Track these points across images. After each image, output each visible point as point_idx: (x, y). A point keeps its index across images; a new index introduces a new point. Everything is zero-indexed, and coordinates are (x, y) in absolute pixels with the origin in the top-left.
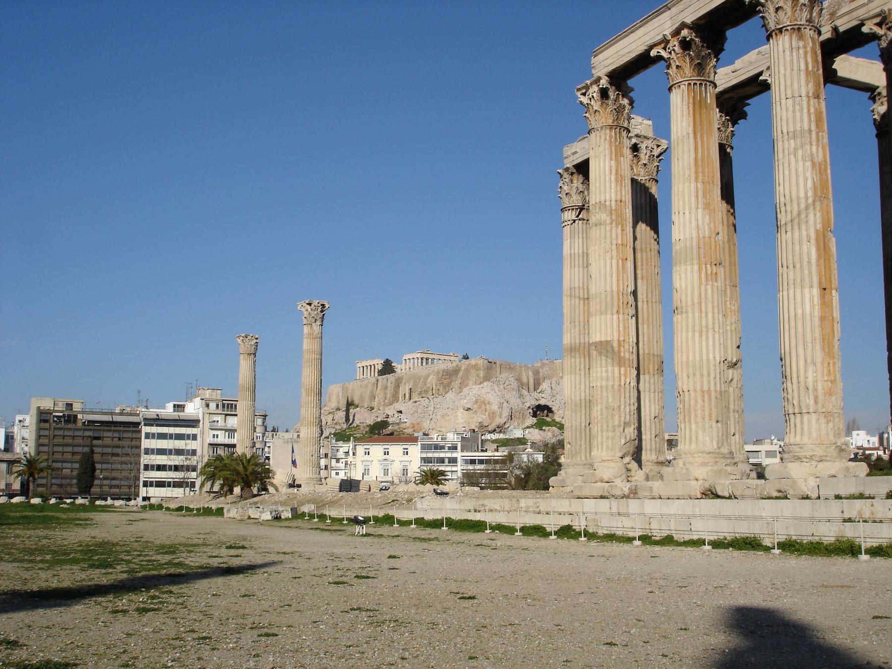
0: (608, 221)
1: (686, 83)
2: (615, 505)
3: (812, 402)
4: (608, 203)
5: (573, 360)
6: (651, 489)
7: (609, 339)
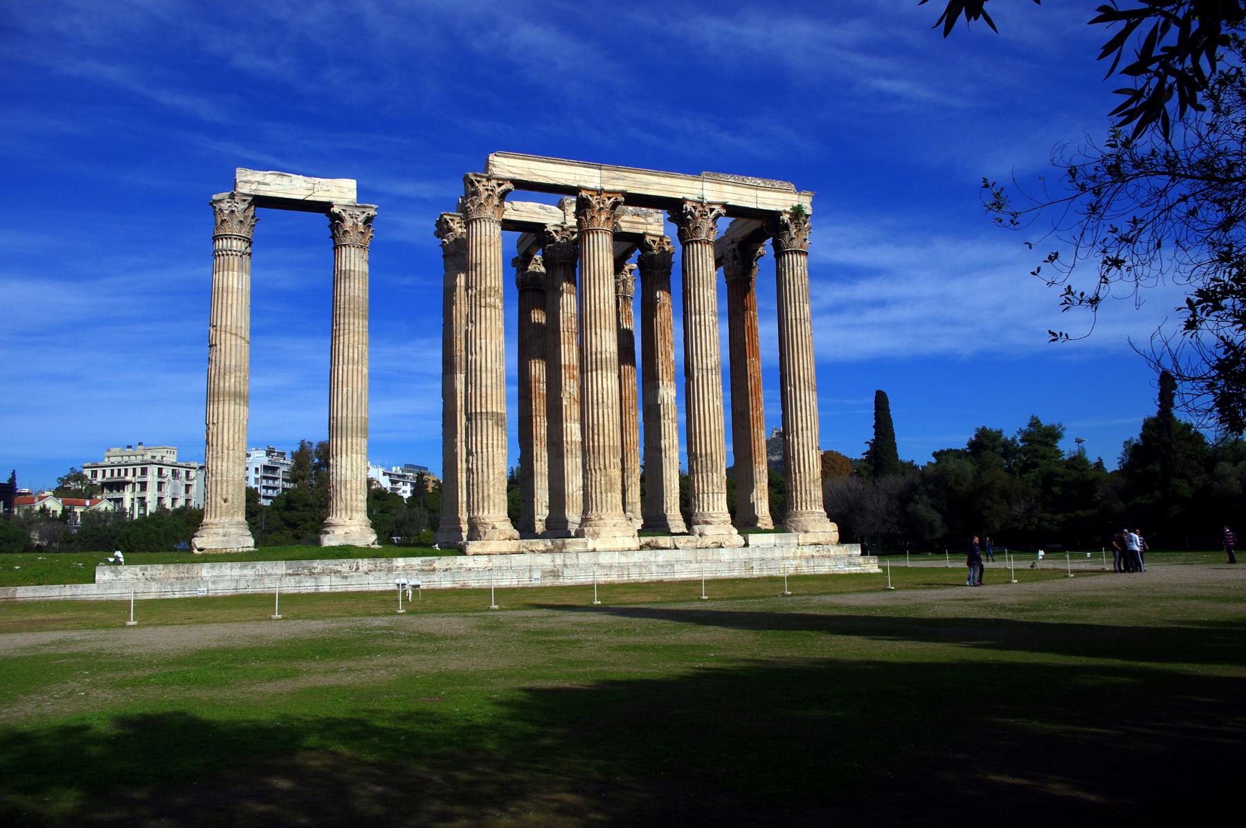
5: (237, 407)
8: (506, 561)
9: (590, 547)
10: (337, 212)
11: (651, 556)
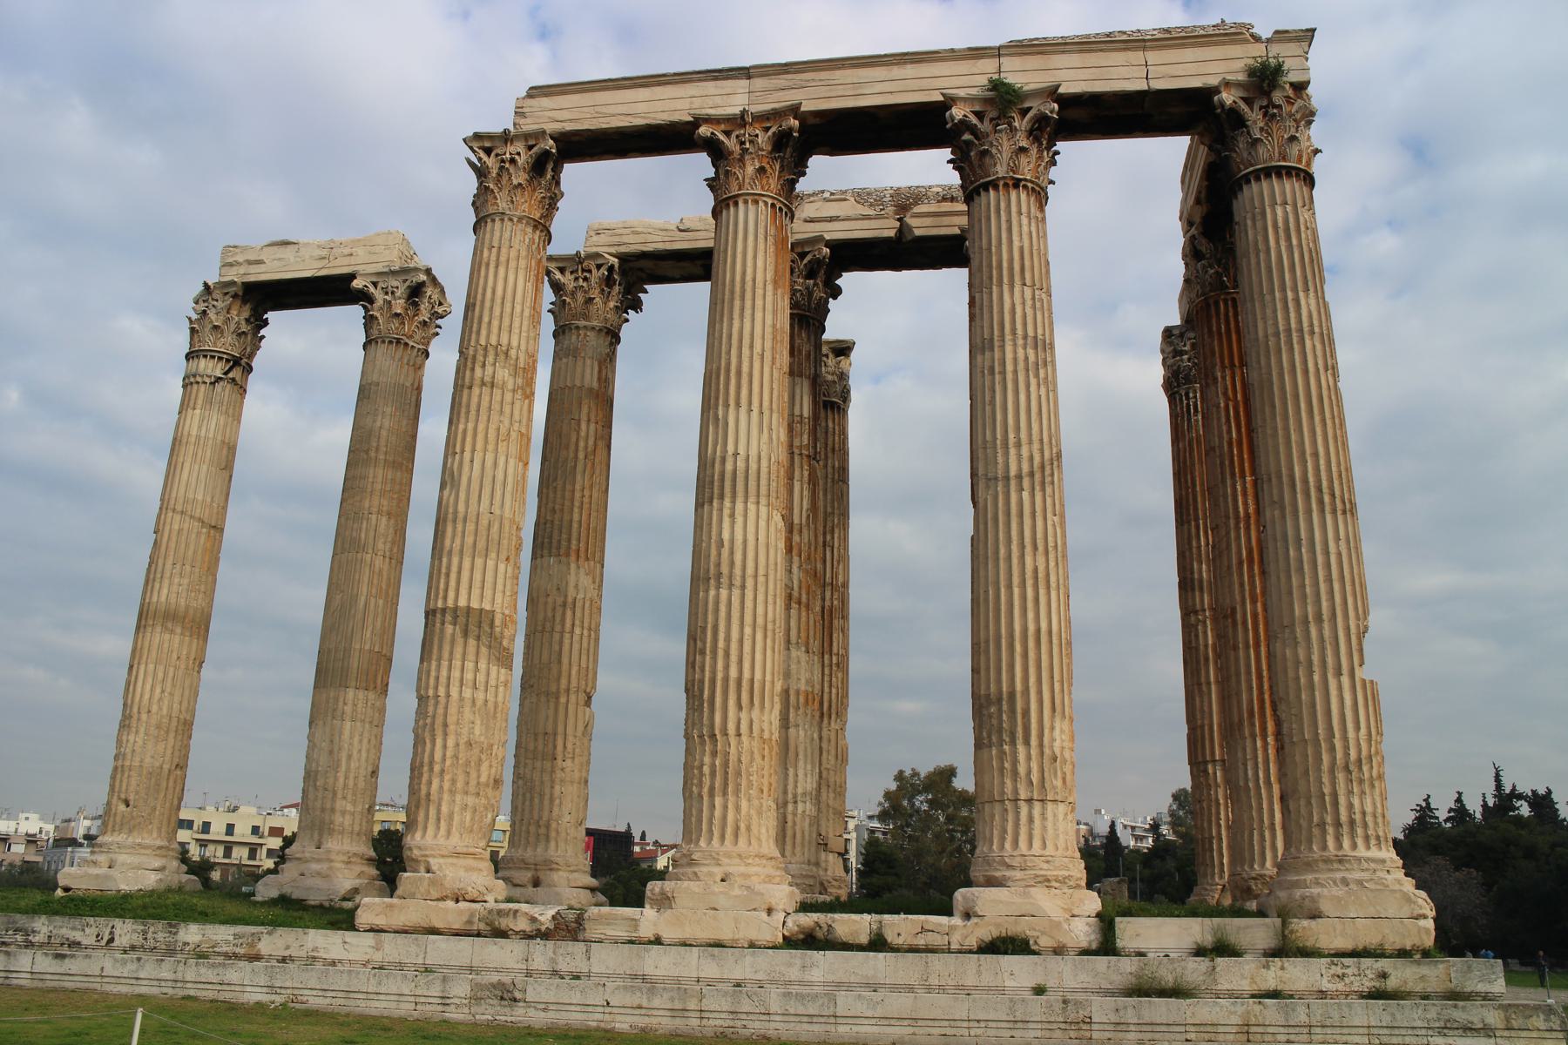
0: (510, 386)
1: (770, 201)
2: (542, 955)
3: (1059, 783)
4: (513, 353)
6: (635, 923)
7: (487, 606)
8: (413, 949)
9: (646, 932)
10: (360, 287)
11: (790, 965)
